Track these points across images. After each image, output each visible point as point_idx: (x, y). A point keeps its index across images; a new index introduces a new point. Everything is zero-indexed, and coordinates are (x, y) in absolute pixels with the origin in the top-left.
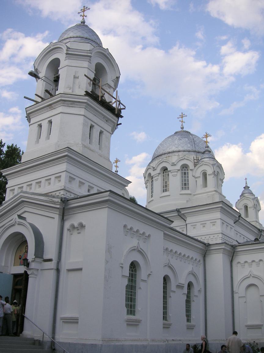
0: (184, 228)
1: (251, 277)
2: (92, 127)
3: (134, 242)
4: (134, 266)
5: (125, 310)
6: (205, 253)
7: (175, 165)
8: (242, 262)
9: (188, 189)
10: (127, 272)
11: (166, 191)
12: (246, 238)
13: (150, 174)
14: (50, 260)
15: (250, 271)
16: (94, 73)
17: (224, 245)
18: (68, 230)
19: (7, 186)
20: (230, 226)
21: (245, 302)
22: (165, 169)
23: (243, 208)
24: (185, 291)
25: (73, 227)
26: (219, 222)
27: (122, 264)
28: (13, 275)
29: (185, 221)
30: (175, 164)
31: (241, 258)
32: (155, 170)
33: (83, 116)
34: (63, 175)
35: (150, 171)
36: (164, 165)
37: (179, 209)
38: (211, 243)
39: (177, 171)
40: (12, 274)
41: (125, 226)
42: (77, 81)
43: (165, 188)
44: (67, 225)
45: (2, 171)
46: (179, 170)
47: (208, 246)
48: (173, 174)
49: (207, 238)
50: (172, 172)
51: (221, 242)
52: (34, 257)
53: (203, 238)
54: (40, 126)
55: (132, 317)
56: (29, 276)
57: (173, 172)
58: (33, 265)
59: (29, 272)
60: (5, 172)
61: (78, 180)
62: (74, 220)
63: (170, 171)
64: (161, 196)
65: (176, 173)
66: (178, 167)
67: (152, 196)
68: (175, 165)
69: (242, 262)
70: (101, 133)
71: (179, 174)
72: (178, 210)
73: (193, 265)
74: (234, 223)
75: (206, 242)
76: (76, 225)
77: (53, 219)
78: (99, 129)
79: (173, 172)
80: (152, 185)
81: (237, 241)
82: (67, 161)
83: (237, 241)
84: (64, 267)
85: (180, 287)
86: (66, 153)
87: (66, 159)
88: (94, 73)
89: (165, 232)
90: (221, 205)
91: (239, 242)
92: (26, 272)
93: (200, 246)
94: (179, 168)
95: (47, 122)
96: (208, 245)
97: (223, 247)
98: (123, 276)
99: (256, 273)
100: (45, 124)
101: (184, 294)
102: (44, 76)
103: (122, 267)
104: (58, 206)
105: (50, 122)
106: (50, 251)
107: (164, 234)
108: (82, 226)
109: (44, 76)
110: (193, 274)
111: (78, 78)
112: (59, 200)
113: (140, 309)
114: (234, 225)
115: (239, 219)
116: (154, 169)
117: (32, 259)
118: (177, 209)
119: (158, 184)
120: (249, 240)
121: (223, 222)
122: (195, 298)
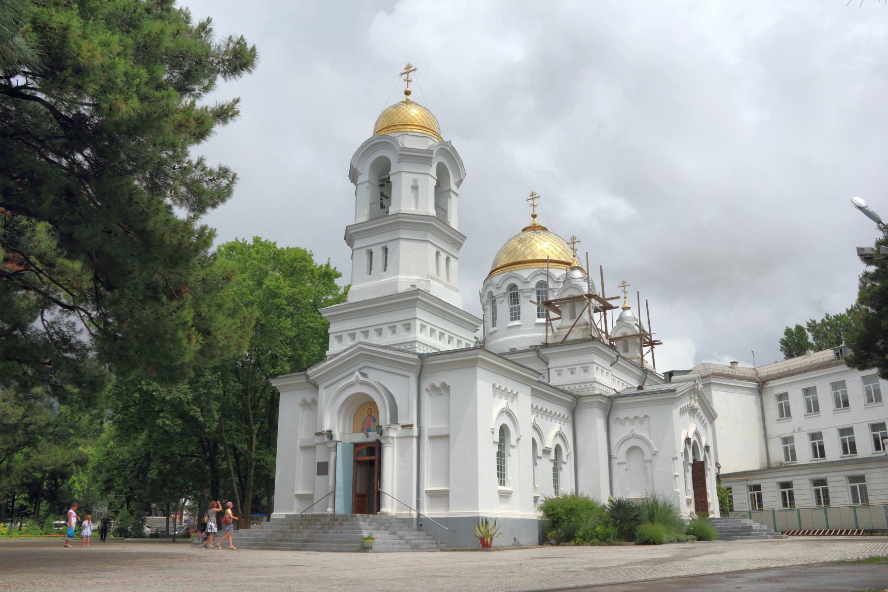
2: (438, 254)
3: (502, 403)
4: (504, 430)
5: (497, 479)
6: (575, 407)
8: (622, 417)
12: (625, 384)
13: (491, 295)
15: (632, 430)
16: (434, 178)
17: (600, 396)
18: (427, 390)
20: (605, 371)
22: (513, 287)
24: (552, 456)
25: (434, 387)
27: (493, 429)
28: (352, 445)
29: (547, 364)
31: (621, 414)
32: (500, 287)
35: (490, 289)
36: (512, 281)
38: (581, 394)
41: (494, 386)
43: (515, 314)
44: (426, 385)
45: (329, 316)
46: (533, 289)
48: (526, 294)
50: (523, 292)
53: (572, 387)
54: (371, 253)
55: (502, 488)
58: (384, 434)
59: (382, 441)
61: (428, 327)
62: (437, 380)
63: (521, 290)
64: (509, 325)
65: (529, 294)
67: (494, 325)
68: (528, 282)
69: (622, 417)
70: (448, 259)
73: (560, 423)
74: (611, 366)
75: (575, 393)
76: (438, 385)
77: (406, 379)
79: (526, 292)
80: (494, 308)
83: (614, 390)
85: (546, 451)
88: (434, 178)
89: (533, 386)
91: (618, 391)
93: (568, 399)
95: (381, 248)
98: (494, 442)
101: (551, 460)
102: (368, 181)
103: (493, 432)
105: (386, 250)
107: (532, 389)
108: (446, 387)
109: (367, 180)
110: (560, 435)
112: (416, 357)
113: (510, 479)
114: (610, 368)
115: (617, 360)
116: (498, 288)
119: (504, 308)
120: (629, 387)
122: (563, 466)
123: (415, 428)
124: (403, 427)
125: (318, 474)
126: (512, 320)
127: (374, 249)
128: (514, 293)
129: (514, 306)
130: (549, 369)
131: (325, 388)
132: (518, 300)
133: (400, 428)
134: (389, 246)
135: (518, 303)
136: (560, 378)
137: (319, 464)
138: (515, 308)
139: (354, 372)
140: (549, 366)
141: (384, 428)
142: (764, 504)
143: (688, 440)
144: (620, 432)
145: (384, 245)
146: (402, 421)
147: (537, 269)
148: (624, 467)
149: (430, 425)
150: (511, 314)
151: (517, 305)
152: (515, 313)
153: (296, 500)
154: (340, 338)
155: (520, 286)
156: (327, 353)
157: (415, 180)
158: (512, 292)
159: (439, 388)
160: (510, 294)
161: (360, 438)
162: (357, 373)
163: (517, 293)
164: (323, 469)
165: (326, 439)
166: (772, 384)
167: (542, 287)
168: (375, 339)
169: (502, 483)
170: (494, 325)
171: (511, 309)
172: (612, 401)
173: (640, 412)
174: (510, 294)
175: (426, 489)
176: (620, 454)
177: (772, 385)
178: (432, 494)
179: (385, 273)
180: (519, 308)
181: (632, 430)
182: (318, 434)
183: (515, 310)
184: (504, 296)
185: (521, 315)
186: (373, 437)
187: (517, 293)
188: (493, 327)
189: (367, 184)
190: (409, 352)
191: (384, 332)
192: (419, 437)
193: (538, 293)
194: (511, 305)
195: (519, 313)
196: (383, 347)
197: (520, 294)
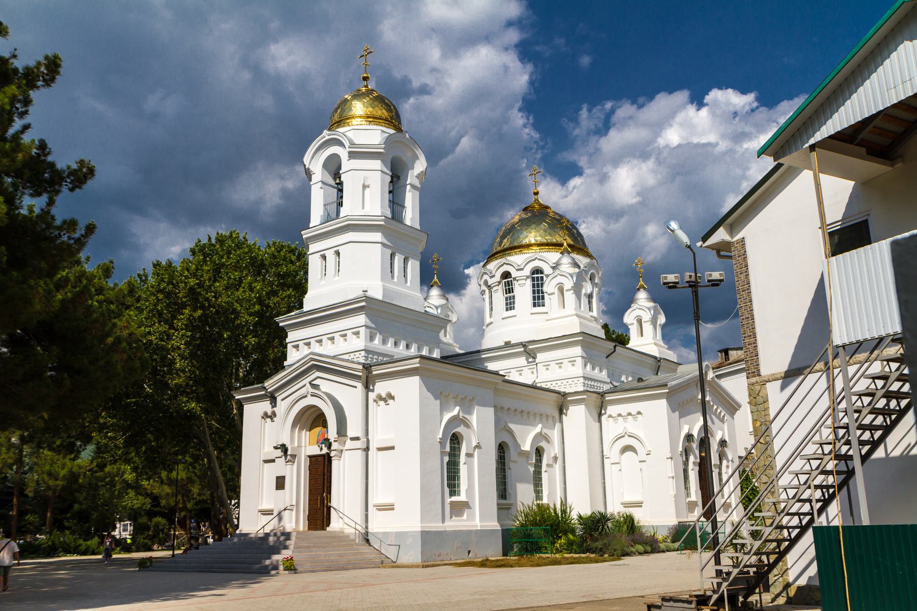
1: (626, 436)
2: (392, 256)
9: (543, 305)
11: (511, 309)
14: (357, 439)
15: (625, 428)
18: (375, 401)
19: (288, 340)
21: (620, 470)
22: (506, 275)
23: (635, 322)
25: (380, 398)
26: (579, 360)
30: (522, 267)
31: (612, 410)
33: (380, 244)
34: (362, 330)
35: (486, 277)
36: (506, 268)
42: (367, 191)
43: (510, 304)
44: (372, 396)
46: (528, 277)
47: (563, 396)
49: (564, 384)
52: (337, 436)
54: (324, 257)
57: (520, 280)
58: (335, 446)
63: (515, 279)
64: (504, 316)
65: (523, 282)
66: (527, 271)
71: (529, 283)
75: (562, 390)
76: (384, 395)
79: (520, 280)
84: (373, 446)
85: (526, 454)
92: (328, 454)
94: (528, 274)
95: (333, 252)
96: (565, 395)
99: (631, 430)
100: (330, 254)
105: (338, 253)
106: (354, 428)
108: (391, 397)
111: (368, 187)
112: (361, 367)
118: (521, 343)
123: (364, 440)
124: (352, 439)
125: (277, 489)
126: (507, 310)
127: (327, 253)
129: (508, 295)
131: (282, 400)
132: (512, 288)
133: (349, 440)
134: (341, 249)
135: (513, 292)
136: (561, 370)
137: (278, 478)
138: (510, 297)
139: (305, 386)
140: (537, 361)
141: (332, 440)
143: (689, 437)
144: (611, 427)
146: (351, 433)
147: (530, 255)
148: (617, 467)
150: (507, 304)
151: (511, 294)
152: (510, 304)
154: (297, 347)
155: (514, 274)
156: (286, 363)
157: (365, 178)
158: (506, 280)
159: (385, 398)
160: (505, 282)
161: (315, 450)
162: (308, 385)
163: (511, 281)
164: (280, 483)
165: (279, 453)
167: (537, 273)
169: (453, 493)
170: (491, 316)
171: (506, 299)
172: (602, 396)
173: (633, 407)
174: (505, 282)
176: (612, 453)
179: (337, 278)
180: (514, 297)
181: (625, 428)
182: (276, 448)
183: (510, 299)
184: (498, 285)
185: (515, 305)
186: (325, 450)
188: (490, 317)
189: (320, 184)
190: (353, 362)
191: (335, 341)
192: (367, 449)
193: (533, 279)
194: (506, 294)
195: (514, 303)
196: (334, 357)
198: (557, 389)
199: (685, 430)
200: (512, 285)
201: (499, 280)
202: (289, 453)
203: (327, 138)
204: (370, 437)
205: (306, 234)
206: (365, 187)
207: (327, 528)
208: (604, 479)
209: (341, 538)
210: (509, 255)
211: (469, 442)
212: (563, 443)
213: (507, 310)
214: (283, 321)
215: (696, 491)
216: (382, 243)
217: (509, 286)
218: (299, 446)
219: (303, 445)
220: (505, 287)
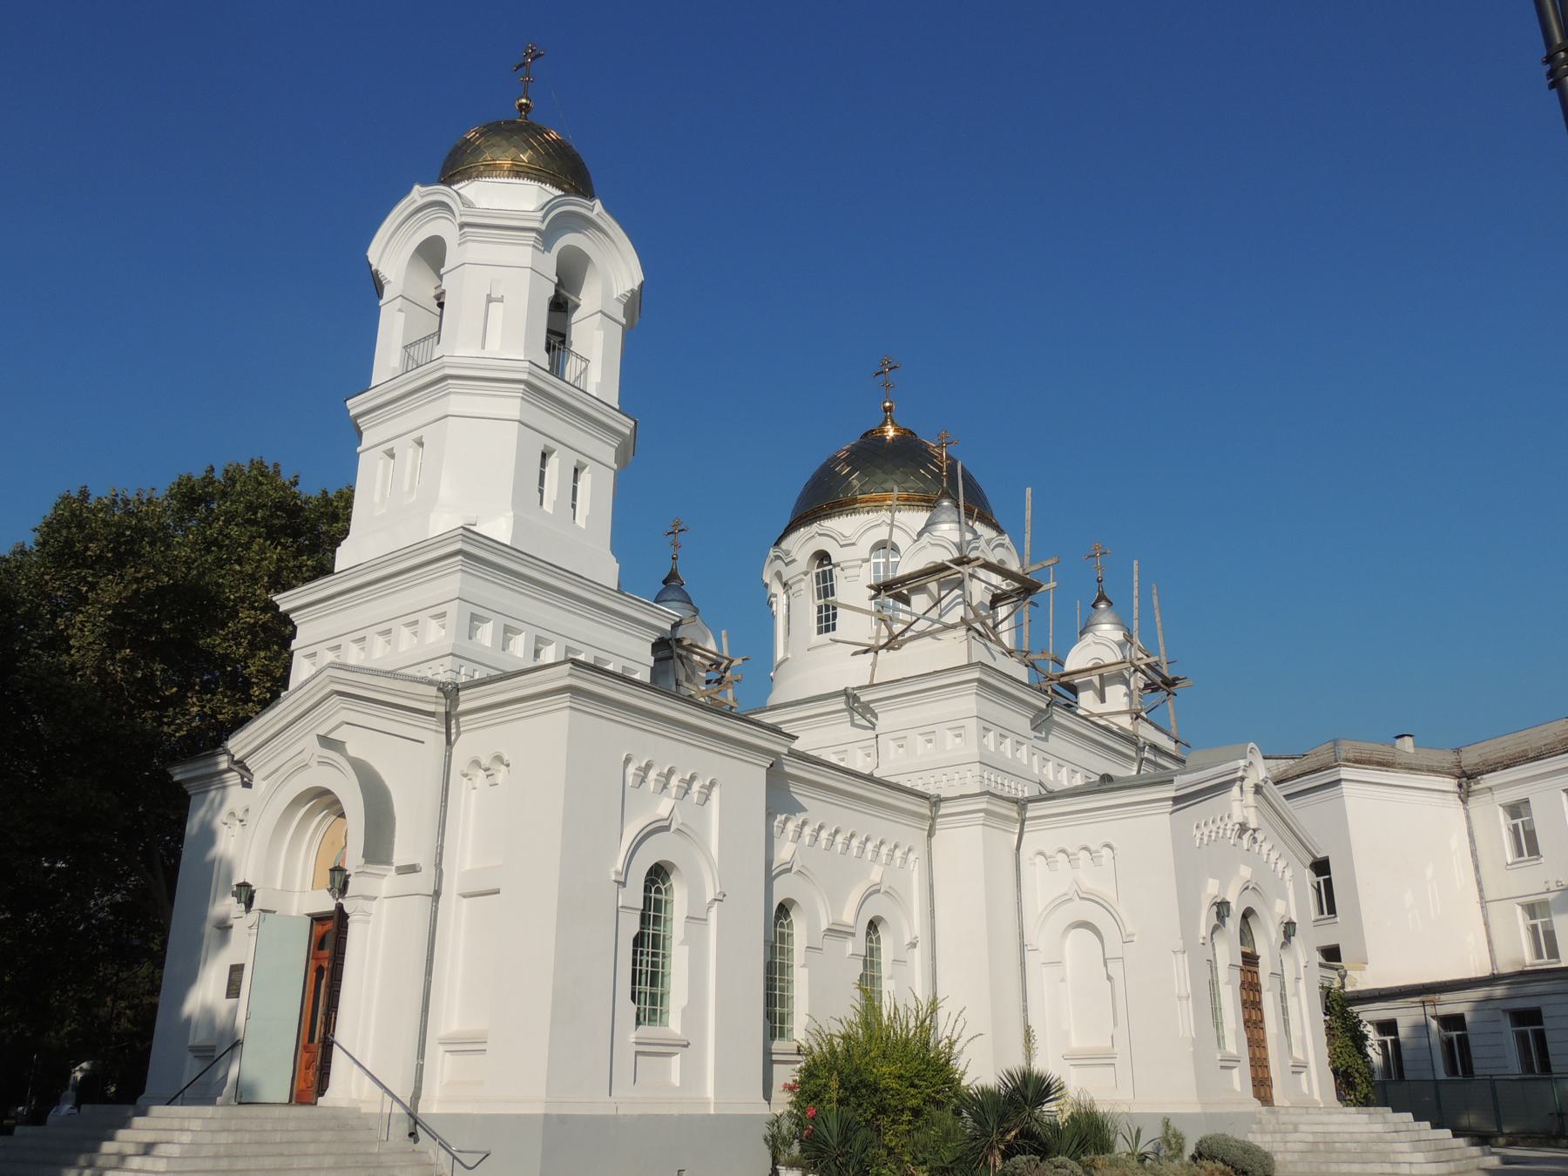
0: (873, 746)
7: (853, 544)
10: (634, 895)
11: (827, 630)
14: (412, 869)
17: (986, 798)
22: (822, 557)
26: (972, 726)
34: (452, 609)
37: (853, 689)
39: (860, 562)
40: (309, 915)
43: (827, 621)
51: (978, 791)
56: (348, 917)
60: (285, 601)
65: (854, 571)
68: (853, 544)
72: (850, 691)
75: (932, 791)
78: (573, 458)
81: (1041, 784)
82: (464, 568)
83: (1041, 784)
84: (451, 887)
86: (458, 546)
87: (460, 563)
90: (976, 674)
96: (936, 802)
97: (984, 806)
99: (1088, 884)
104: (430, 708)
106: (407, 844)
111: (501, 300)
112: (433, 691)
117: (358, 867)
118: (846, 690)
121: (986, 725)
123: (428, 872)
126: (820, 632)
128: (824, 572)
130: (877, 736)
132: (832, 586)
134: (425, 433)
135: (833, 595)
142: (1476, 1064)
145: (416, 435)
146: (400, 856)
149: (463, 861)
150: (820, 620)
153: (190, 1056)
158: (820, 570)
160: (817, 575)
166: (1489, 780)
168: (354, 656)
174: (818, 573)
175: (442, 1032)
177: (1489, 784)
178: (468, 1045)
185: (837, 621)
187: (830, 571)
194: (819, 598)
196: (392, 674)
197: (836, 571)
198: (920, 788)
199: (1212, 889)
200: (831, 580)
201: (804, 568)
202: (257, 904)
203: (420, 202)
204: (444, 867)
205: (355, 405)
206: (490, 299)
207: (320, 1099)
208: (1025, 1000)
209: (346, 1123)
210: (828, 516)
211: (696, 891)
212: (933, 916)
213: (820, 632)
214: (285, 601)
215: (1236, 1033)
216: (520, 422)
217: (825, 581)
218: (287, 890)
219: (297, 888)
220: (818, 583)
